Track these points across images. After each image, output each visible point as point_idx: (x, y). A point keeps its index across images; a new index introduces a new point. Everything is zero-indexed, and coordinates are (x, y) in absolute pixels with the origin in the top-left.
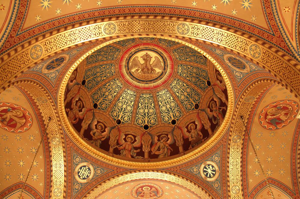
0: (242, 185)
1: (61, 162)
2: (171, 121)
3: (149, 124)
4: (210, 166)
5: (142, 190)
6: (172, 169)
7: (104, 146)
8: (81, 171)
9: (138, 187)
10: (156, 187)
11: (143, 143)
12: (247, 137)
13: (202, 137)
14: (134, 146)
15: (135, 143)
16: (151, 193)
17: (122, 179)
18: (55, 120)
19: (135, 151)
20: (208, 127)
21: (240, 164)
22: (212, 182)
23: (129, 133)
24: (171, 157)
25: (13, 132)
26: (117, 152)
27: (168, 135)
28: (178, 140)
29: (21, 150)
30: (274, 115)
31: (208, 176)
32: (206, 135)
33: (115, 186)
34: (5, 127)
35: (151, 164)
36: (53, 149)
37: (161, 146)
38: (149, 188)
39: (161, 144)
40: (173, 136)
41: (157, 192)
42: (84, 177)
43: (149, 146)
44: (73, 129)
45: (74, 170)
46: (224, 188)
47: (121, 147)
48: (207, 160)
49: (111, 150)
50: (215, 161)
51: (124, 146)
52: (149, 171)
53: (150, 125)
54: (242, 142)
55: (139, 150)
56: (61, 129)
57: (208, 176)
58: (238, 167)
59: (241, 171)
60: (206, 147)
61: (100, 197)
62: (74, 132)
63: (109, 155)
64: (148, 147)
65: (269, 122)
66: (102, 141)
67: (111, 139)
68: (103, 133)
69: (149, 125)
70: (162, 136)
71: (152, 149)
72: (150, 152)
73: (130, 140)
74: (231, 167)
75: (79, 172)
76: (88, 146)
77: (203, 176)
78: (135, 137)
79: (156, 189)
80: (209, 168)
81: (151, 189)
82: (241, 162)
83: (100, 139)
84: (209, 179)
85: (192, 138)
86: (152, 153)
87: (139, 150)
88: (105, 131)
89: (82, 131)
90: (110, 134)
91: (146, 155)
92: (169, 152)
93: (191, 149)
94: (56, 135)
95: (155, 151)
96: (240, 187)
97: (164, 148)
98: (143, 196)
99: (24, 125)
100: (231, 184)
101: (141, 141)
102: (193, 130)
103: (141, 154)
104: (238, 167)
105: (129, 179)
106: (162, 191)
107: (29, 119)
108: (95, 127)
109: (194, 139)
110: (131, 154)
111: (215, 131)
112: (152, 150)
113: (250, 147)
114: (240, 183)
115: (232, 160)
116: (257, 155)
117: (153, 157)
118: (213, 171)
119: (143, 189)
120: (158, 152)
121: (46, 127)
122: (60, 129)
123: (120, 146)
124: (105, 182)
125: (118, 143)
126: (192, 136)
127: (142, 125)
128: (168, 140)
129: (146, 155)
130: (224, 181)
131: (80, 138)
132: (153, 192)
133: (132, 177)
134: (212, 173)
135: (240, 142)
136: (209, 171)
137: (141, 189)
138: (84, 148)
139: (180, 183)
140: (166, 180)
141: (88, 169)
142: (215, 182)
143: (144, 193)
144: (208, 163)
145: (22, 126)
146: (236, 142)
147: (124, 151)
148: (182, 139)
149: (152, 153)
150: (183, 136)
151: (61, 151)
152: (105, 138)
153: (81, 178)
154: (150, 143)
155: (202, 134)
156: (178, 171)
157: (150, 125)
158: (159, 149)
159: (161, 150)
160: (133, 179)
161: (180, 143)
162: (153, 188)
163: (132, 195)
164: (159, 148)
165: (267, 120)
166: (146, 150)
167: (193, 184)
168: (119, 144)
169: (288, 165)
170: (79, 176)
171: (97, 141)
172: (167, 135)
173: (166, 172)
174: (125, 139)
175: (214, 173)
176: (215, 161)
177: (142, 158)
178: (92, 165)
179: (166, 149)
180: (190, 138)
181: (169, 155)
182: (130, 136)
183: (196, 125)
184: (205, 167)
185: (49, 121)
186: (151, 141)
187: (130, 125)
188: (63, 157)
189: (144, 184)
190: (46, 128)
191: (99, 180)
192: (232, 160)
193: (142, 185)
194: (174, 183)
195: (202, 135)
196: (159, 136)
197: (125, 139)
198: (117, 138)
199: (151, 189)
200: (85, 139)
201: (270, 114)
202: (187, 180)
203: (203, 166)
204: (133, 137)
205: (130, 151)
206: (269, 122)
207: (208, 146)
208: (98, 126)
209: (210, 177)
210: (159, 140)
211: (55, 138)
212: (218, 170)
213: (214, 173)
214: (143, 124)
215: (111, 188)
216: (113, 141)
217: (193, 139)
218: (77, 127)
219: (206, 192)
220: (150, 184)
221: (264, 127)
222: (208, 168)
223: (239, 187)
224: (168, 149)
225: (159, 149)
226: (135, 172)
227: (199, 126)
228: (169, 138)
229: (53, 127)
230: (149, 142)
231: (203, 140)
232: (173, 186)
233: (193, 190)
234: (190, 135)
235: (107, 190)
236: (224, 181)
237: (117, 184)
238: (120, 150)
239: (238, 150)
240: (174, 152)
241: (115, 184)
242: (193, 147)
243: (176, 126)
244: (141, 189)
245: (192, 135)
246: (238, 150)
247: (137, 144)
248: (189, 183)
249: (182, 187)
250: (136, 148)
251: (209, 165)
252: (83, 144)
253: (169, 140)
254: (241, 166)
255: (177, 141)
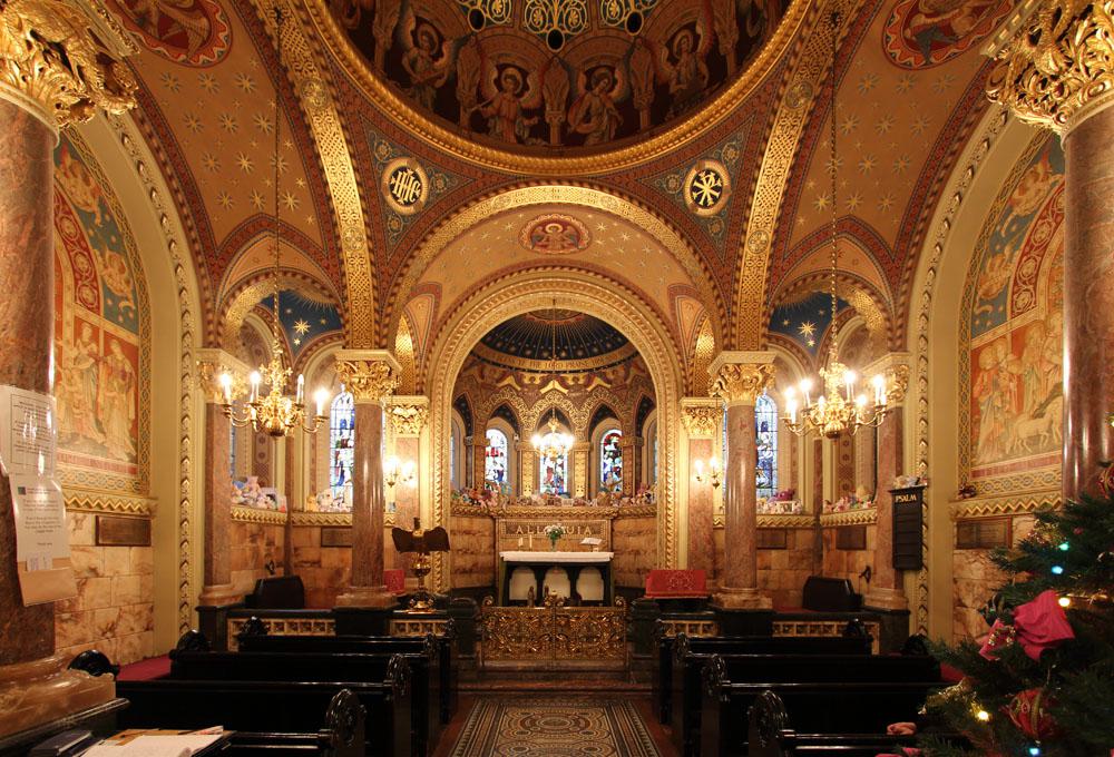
0: (776, 232)
1: (342, 158)
2: (626, 18)
3: (563, 29)
4: (712, 176)
5: (544, 230)
6: (617, 180)
7: (444, 107)
8: (398, 183)
9: (533, 223)
10: (577, 223)
11: (546, 96)
12: (828, 91)
13: (706, 82)
14: (524, 105)
15: (527, 94)
16: (564, 240)
17: (495, 203)
18: (294, 19)
19: (526, 122)
20: (729, 47)
21: (787, 174)
22: (707, 219)
23: (509, 61)
24: (621, 142)
25: (185, 63)
26: (479, 128)
27: (614, 69)
28: (639, 89)
29: (229, 124)
30: (936, 14)
31: (701, 203)
32: (719, 75)
33: (482, 222)
34: (158, 46)
35: (566, 164)
36: (315, 118)
37: (593, 109)
38: (560, 227)
39: (593, 100)
40: (628, 72)
41: (577, 236)
42: (406, 199)
43: (563, 107)
44: (354, 51)
45: (380, 179)
46: (733, 236)
47: (490, 109)
48: (707, 158)
49: (465, 118)
50: (726, 162)
51: (496, 104)
52: (560, 182)
53: (567, 31)
54: (810, 105)
55: (535, 120)
56: (319, 53)
57: (701, 203)
58: (779, 182)
59: (785, 193)
60: (712, 116)
61: (450, 250)
62: (358, 62)
63: (460, 136)
64: (558, 110)
65: (914, 38)
66: (438, 90)
67: (460, 84)
68: (437, 60)
69: (563, 33)
70: (597, 73)
71: (571, 117)
72: (564, 126)
73: (512, 86)
74: (762, 180)
75: (392, 187)
76: (404, 107)
77: (690, 201)
78: (525, 74)
79: (577, 230)
80: (707, 179)
81: (564, 229)
82: (792, 168)
83: (431, 82)
84: (701, 212)
85: (679, 82)
86: (570, 130)
87: (535, 120)
88: (442, 55)
89: (379, 55)
90: (455, 63)
91: (554, 133)
92: (614, 127)
93: (670, 119)
94: (310, 74)
95: (577, 122)
96: (770, 235)
97: (601, 114)
98: (545, 246)
99: (208, 37)
100: (751, 227)
101: (541, 88)
102: (684, 55)
103: (541, 131)
104: (779, 182)
105: (512, 205)
106: (590, 235)
107: (217, 16)
108: (411, 39)
109: (684, 87)
110: (517, 130)
111: (744, 63)
112: (569, 120)
113: (828, 126)
115: (770, 161)
116: (836, 147)
117: (573, 143)
118: (714, 189)
119: (547, 228)
120: (585, 125)
121: (275, 44)
122: (317, 53)
123: (486, 106)
124: (457, 212)
125: (480, 97)
126: (677, 75)
127: (544, 30)
128: (611, 89)
129: (554, 133)
130: (736, 219)
131: (377, 82)
132: (569, 236)
133: (519, 198)
134: (712, 196)
135: (805, 104)
136: (706, 189)
137: (541, 228)
138: (395, 113)
139: (631, 218)
140: (602, 207)
141: (412, 178)
142: (714, 219)
143: (548, 240)
144: (708, 165)
145: (204, 42)
146: (792, 106)
147: (498, 123)
148: (650, 87)
149: (570, 130)
150: (655, 75)
151: (336, 127)
152: (446, 77)
153: (401, 201)
154: (564, 97)
155: (710, 70)
156: (631, 185)
157: (567, 31)
158: (587, 119)
159: (593, 120)
160: (524, 204)
161: (643, 100)
162: (568, 227)
163: (521, 242)
164: (588, 112)
165: (908, 33)
166: (554, 117)
167: (661, 222)
168: (484, 100)
169: (911, 185)
170: (396, 198)
171: (424, 89)
172: (612, 70)
173: (601, 189)
174: (498, 82)
175: (717, 194)
176: (726, 162)
177: (544, 143)
178: (422, 165)
179: (606, 118)
180: (674, 83)
181: (612, 136)
182: (511, 71)
183: (697, 38)
184: (698, 179)
185: (277, 21)
186: (567, 89)
187: (508, 31)
188: (345, 145)
189: (549, 217)
190: (276, 48)
191: (443, 205)
192: (770, 161)
193: (543, 218)
194: (617, 217)
195: (707, 76)
196: (589, 74)
197: (498, 82)
198: (477, 79)
199: (564, 229)
200: (391, 83)
201: (927, 10)
202: (649, 209)
203: (693, 173)
204: (519, 77)
205: (513, 122)
206: (914, 38)
207: (717, 112)
208: (419, 34)
209: (705, 205)
210: (589, 87)
211: (308, 81)
212: (729, 188)
213: (717, 194)
214: (548, 29)
215: (473, 227)
216: (467, 87)
217: (681, 86)
218: (362, 40)
219: (689, 244)
220: (562, 217)
221: (891, 58)
222: (704, 179)
223: (767, 237)
224: (610, 118)
225: (587, 119)
226: (528, 185)
227: (704, 43)
228: (615, 82)
229: (294, 43)
230: (561, 94)
231: (707, 93)
232: (615, 224)
233: (660, 237)
234: (674, 74)
235: (465, 232)
236: (736, 219)
237: (486, 215)
238: (487, 120)
239: (793, 132)
240: (628, 129)
241: (483, 217)
242: (676, 114)
243: (638, 36)
244: (541, 228)
245: (679, 72)
246: (793, 132)
247: (529, 100)
248: (653, 219)
249: (636, 226)
250: (528, 113)
251: (708, 172)
252: (388, 98)
253: (617, 87)
254: (788, 181)
255: (636, 92)
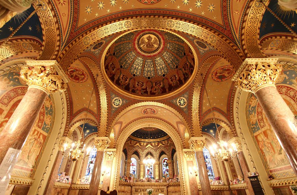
5: (147, 110)
9: (144, 109)
11: (147, 86)
19: (143, 91)
21: (199, 100)
26: (133, 92)
31: (181, 105)
33: (133, 109)
39: (157, 87)
49: (130, 90)
51: (137, 88)
52: (150, 101)
54: (201, 88)
55: (145, 90)
57: (181, 105)
58: (197, 101)
72: (151, 91)
74: (193, 100)
75: (114, 102)
78: (143, 83)
81: (151, 110)
86: (152, 92)
87: (145, 90)
91: (149, 93)
92: (161, 91)
97: (158, 90)
98: (147, 114)
103: (146, 92)
104: (197, 101)
105: (140, 105)
106: (157, 111)
113: (205, 91)
114: (198, 109)
115: (195, 97)
117: (152, 94)
128: (160, 85)
129: (149, 93)
132: (153, 111)
136: (182, 102)
139: (166, 108)
156: (165, 102)
160: (142, 105)
163: (142, 113)
166: (149, 90)
167: (173, 109)
170: (115, 104)
172: (160, 82)
182: (140, 83)
192: (195, 97)
193: (146, 108)
196: (156, 83)
199: (151, 110)
202: (170, 106)
209: (182, 105)
210: (156, 85)
226: (143, 102)
228: (161, 84)
233: (173, 111)
238: (135, 91)
241: (133, 108)
247: (144, 87)
248: (171, 108)
249: (167, 109)
250: (143, 89)
